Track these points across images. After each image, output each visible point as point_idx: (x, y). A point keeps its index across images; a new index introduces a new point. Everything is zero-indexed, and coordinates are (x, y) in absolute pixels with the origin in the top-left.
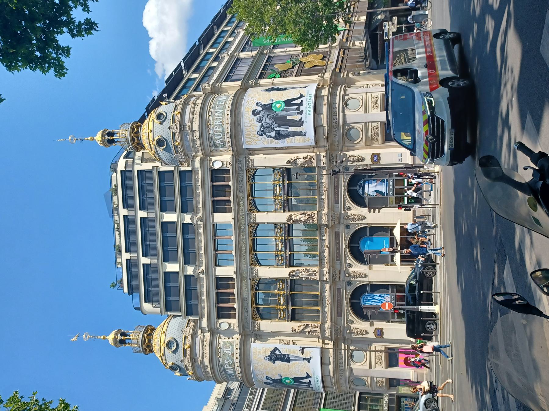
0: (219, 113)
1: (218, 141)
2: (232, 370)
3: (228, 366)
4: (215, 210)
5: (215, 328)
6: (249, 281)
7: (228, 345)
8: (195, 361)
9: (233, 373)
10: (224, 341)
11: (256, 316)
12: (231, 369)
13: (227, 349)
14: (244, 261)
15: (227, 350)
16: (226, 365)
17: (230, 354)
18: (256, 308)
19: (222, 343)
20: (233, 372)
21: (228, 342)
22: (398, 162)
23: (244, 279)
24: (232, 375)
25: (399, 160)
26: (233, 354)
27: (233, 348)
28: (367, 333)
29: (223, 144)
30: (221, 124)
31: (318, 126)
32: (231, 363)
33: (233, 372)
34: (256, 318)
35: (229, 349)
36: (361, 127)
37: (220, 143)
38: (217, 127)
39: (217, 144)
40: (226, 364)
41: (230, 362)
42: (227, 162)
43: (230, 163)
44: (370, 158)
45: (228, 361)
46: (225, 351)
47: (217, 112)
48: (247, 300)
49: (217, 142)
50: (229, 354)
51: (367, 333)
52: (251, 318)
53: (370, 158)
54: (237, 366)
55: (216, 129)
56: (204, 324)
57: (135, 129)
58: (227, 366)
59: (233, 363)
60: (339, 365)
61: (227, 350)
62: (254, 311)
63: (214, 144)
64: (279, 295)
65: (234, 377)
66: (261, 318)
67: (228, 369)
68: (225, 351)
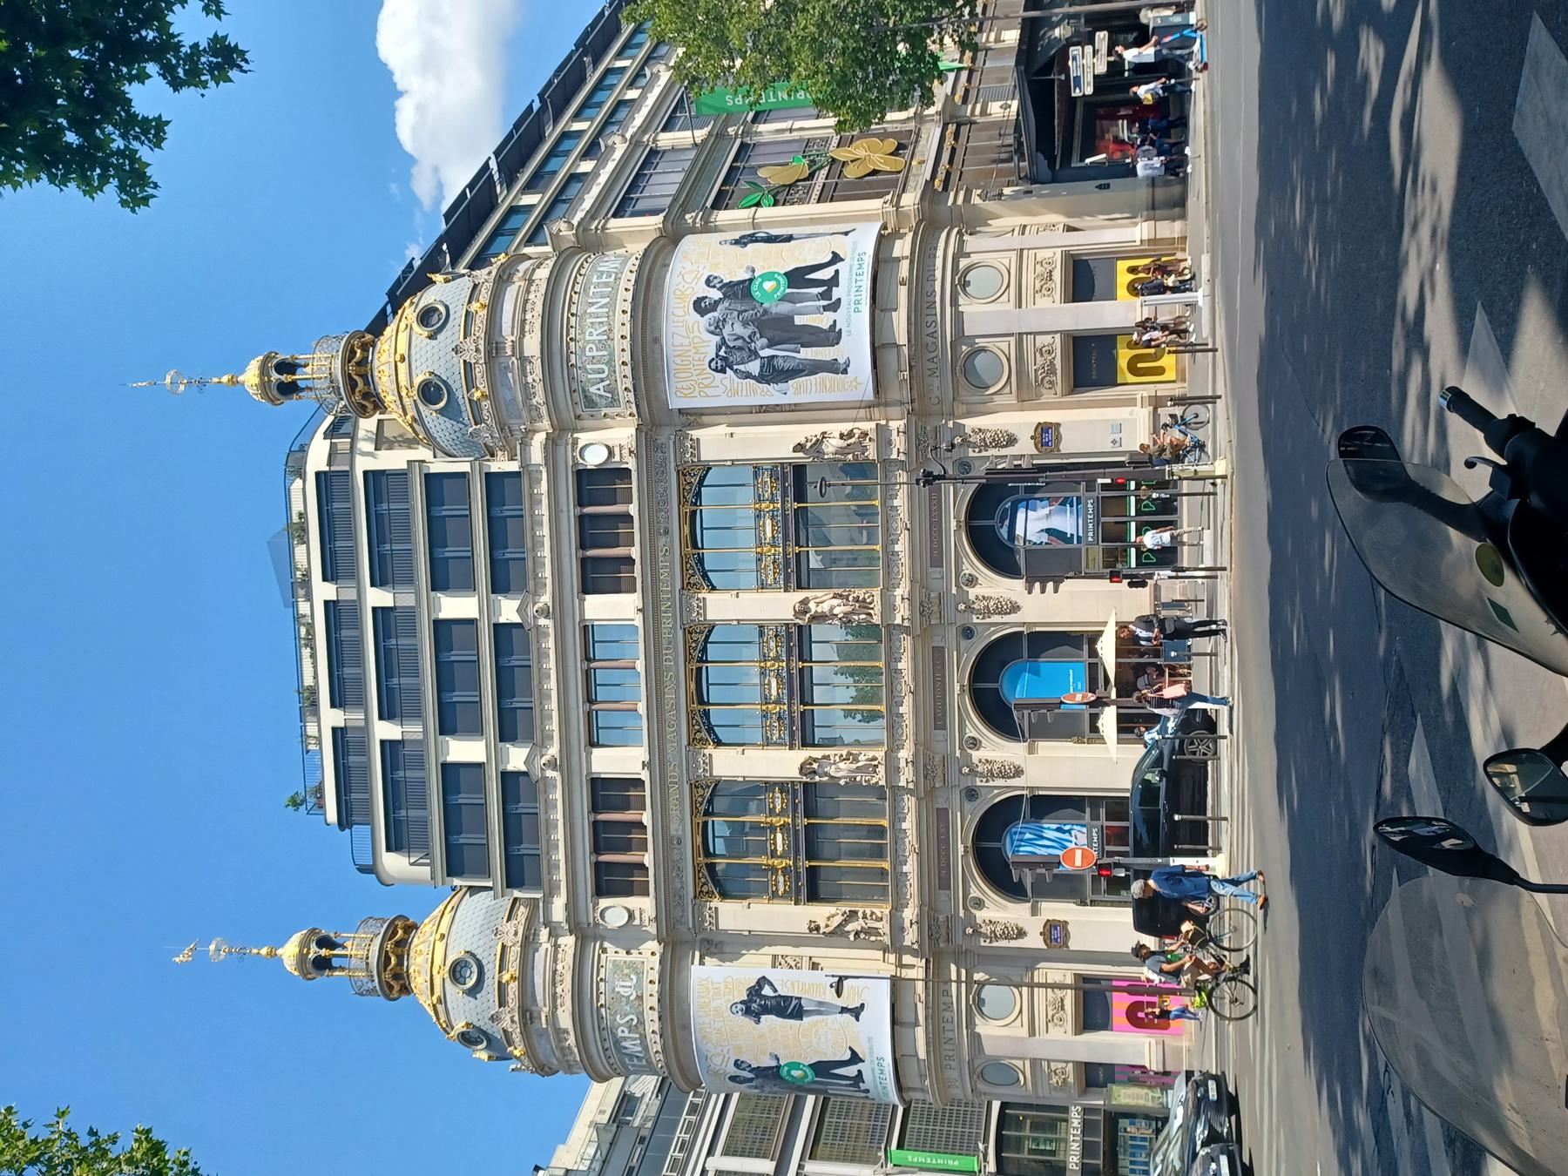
0: (601, 307)
1: (597, 387)
2: (639, 1042)
3: (626, 1031)
4: (588, 587)
5: (589, 924)
6: (687, 787)
7: (626, 971)
8: (531, 1018)
10: (615, 961)
11: (705, 889)
12: (636, 1039)
13: (623, 984)
14: (673, 732)
15: (623, 986)
16: (619, 1030)
17: (632, 998)
18: (706, 864)
19: (610, 966)
20: (640, 1049)
21: (625, 962)
22: (1109, 449)
23: (673, 783)
24: (637, 1057)
25: (1114, 442)
26: (640, 998)
27: (639, 980)
28: (1021, 934)
29: (610, 395)
30: (606, 337)
31: (883, 346)
32: (635, 1023)
33: (640, 1049)
34: (707, 893)
35: (629, 984)
36: (1004, 346)
37: (602, 392)
38: (594, 348)
39: (594, 397)
40: (622, 1025)
41: (632, 1020)
42: (621, 447)
43: (631, 452)
44: (1032, 438)
45: (626, 1016)
46: (617, 989)
47: (592, 304)
48: (680, 841)
49: (593, 389)
50: (629, 997)
51: (1021, 934)
52: (691, 895)
53: (1032, 438)
54: (653, 1032)
55: (591, 354)
56: (558, 911)
57: (356, 353)
58: (623, 1032)
59: (641, 1022)
60: (942, 1025)
61: (623, 986)
62: (701, 875)
63: (585, 396)
64: (773, 828)
65: (644, 1062)
66: (720, 894)
67: (625, 1039)
68: (617, 989)
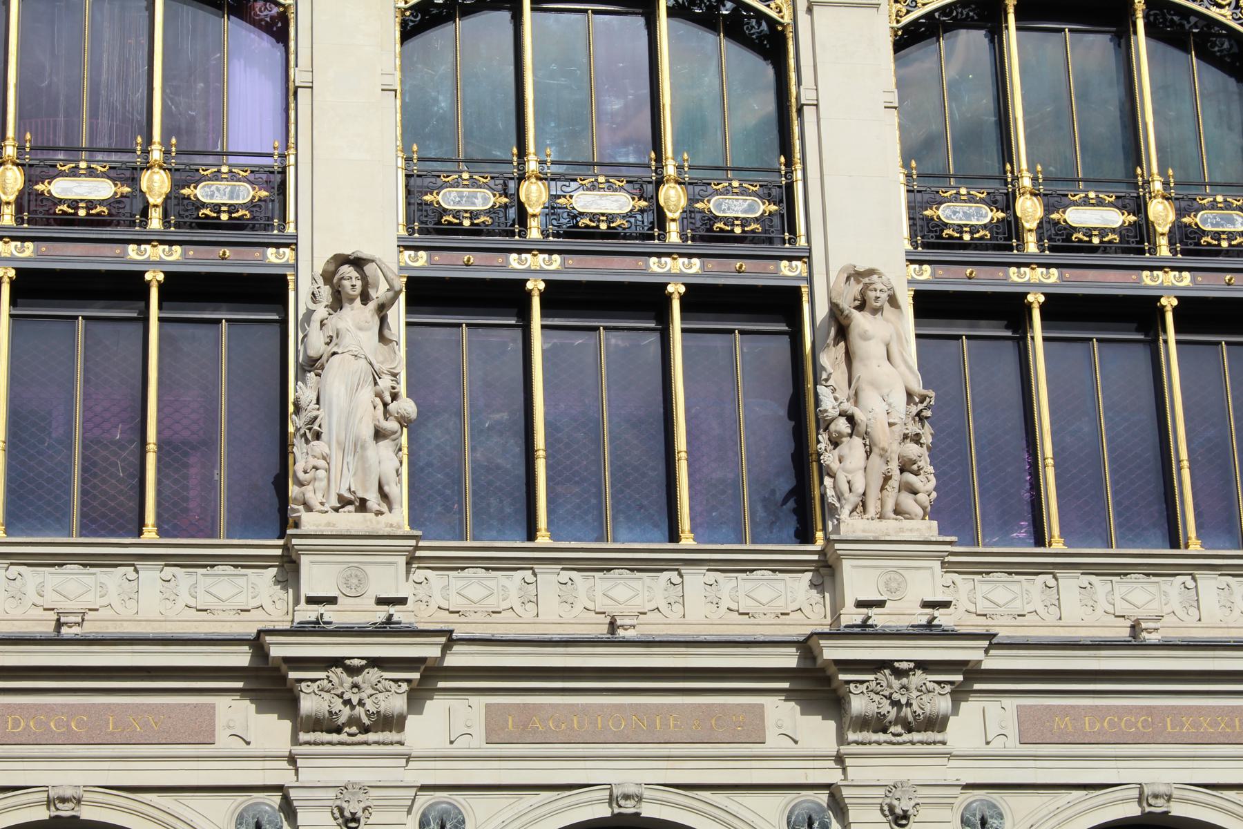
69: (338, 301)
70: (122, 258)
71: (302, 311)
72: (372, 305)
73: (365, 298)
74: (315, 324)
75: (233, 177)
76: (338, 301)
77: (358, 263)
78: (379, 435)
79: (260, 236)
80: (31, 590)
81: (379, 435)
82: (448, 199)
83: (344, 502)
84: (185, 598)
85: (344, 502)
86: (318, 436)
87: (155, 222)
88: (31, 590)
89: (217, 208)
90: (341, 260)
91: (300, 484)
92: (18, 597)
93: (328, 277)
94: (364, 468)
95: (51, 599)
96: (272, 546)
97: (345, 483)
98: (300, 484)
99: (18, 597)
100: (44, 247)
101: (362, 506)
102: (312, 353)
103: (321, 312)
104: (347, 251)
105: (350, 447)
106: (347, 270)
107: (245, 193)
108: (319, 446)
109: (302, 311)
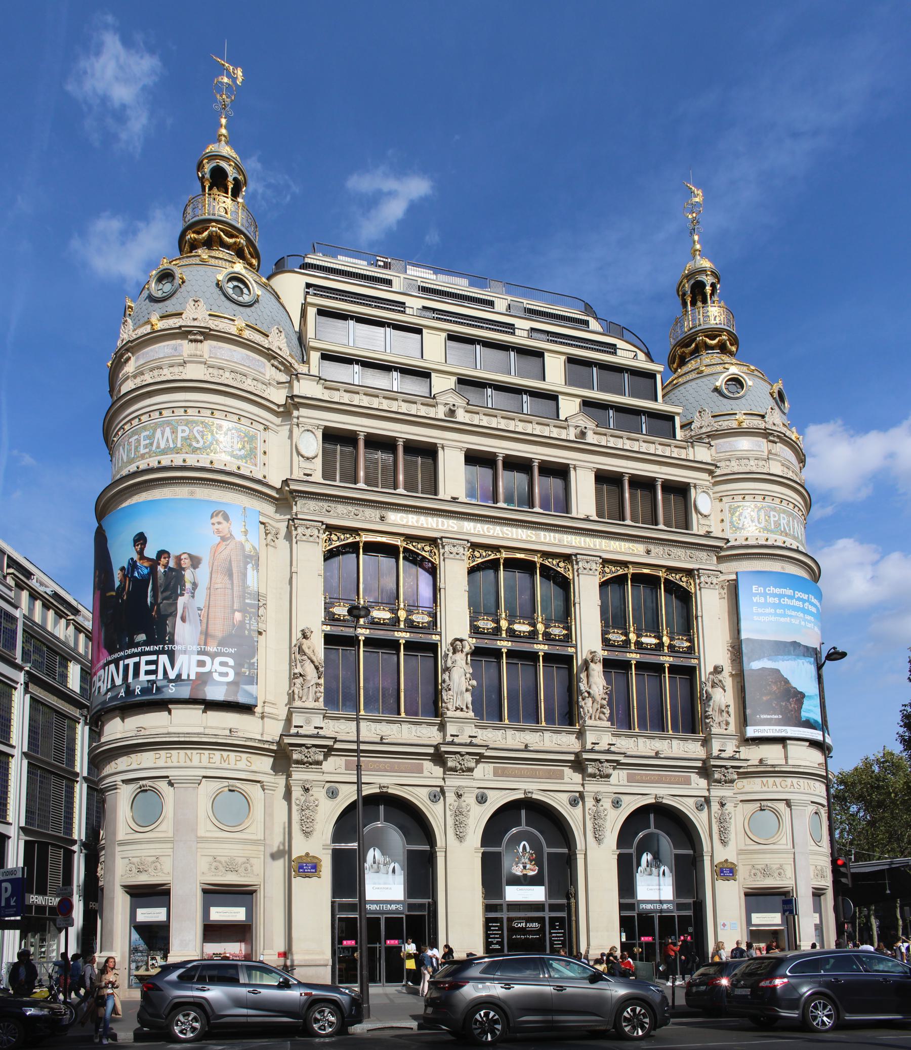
7: (248, 447)
9: (158, 447)
20: (162, 446)
21: (256, 448)
22: (720, 922)
23: (437, 523)
24: (151, 444)
25: (724, 925)
31: (785, 747)
42: (710, 526)
43: (709, 532)
44: (307, 854)
53: (307, 854)
55: (772, 516)
58: (183, 431)
65: (142, 451)
66: (330, 551)
69: (454, 653)
70: (393, 636)
71: (443, 654)
72: (464, 653)
73: (462, 651)
74: (449, 658)
75: (423, 613)
76: (454, 653)
77: (461, 640)
78: (467, 690)
79: (431, 631)
80: (373, 729)
81: (467, 690)
82: (481, 624)
83: (457, 709)
84: (414, 733)
85: (457, 709)
86: (450, 690)
87: (402, 626)
88: (373, 729)
89: (418, 622)
90: (456, 640)
91: (446, 703)
92: (370, 731)
93: (452, 644)
94: (463, 700)
95: (378, 732)
96: (438, 720)
97: (459, 703)
98: (446, 703)
99: (370, 731)
100: (372, 631)
101: (462, 710)
102: (448, 666)
103: (450, 654)
104: (458, 637)
105: (459, 693)
106: (458, 643)
107: (427, 619)
108: (450, 693)
109: (443, 654)
